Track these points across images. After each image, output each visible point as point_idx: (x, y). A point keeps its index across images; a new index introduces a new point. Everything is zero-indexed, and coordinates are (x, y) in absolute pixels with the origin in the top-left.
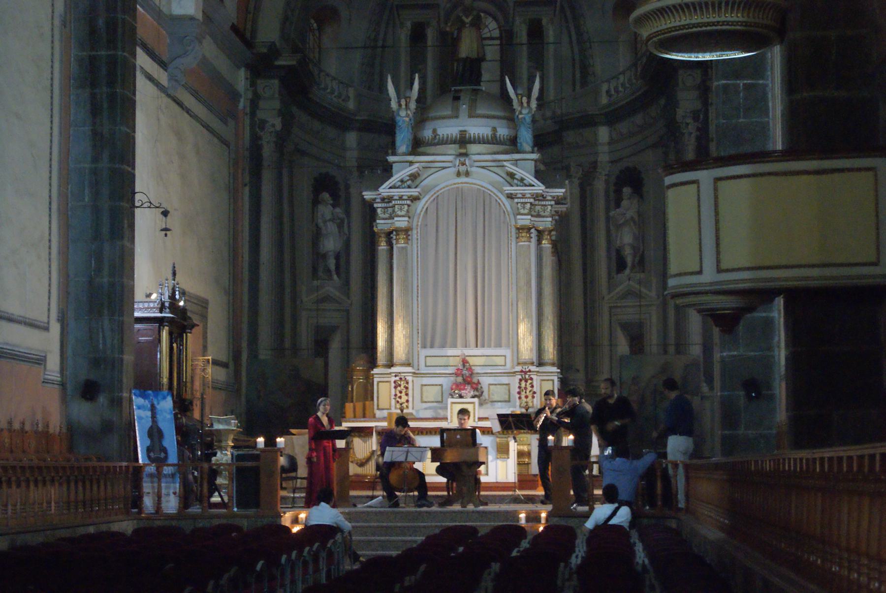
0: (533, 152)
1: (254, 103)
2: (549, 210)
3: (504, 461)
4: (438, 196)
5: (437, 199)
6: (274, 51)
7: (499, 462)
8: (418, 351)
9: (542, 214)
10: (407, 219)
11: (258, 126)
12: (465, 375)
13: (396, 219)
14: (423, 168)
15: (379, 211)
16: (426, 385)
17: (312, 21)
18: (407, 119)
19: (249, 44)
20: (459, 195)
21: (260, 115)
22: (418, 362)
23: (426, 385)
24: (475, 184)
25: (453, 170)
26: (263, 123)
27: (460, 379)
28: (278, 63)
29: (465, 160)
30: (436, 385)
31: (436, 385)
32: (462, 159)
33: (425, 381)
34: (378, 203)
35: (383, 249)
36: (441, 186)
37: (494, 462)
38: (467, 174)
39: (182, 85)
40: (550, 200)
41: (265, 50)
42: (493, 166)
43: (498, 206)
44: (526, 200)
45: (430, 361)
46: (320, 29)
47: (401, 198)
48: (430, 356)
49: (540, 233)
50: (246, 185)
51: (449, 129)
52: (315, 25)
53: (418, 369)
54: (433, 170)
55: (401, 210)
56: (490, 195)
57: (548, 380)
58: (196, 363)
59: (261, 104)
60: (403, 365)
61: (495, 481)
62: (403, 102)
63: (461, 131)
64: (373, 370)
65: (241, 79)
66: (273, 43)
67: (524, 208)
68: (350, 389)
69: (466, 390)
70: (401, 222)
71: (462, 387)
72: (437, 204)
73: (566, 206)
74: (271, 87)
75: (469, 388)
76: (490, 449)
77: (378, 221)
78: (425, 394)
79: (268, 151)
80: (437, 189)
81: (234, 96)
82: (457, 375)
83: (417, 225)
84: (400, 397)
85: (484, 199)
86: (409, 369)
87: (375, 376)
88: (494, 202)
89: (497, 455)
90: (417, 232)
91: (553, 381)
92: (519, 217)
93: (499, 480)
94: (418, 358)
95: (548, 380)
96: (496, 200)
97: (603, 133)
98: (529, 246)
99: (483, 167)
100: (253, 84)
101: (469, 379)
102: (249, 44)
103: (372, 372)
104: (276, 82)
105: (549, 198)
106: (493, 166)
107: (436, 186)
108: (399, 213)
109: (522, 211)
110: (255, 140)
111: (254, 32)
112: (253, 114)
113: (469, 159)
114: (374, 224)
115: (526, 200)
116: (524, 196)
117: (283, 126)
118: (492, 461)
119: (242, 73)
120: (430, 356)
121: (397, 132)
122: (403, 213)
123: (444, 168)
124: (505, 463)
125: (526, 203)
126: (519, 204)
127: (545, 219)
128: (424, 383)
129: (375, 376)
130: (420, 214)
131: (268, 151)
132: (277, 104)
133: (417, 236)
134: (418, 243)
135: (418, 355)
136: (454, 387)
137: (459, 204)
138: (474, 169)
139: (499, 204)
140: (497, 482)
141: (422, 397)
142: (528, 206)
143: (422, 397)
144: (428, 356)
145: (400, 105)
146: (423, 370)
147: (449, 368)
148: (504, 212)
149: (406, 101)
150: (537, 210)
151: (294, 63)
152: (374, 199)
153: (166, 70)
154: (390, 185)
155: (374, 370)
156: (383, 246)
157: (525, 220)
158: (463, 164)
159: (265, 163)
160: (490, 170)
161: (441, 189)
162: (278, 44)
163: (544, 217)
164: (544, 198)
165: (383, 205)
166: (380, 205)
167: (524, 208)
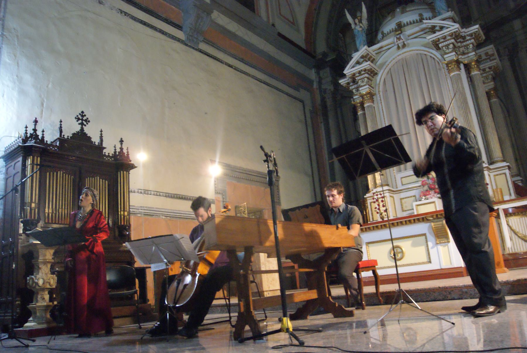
0: (448, 11)
1: (320, 83)
2: (471, 47)
3: (444, 246)
4: (390, 69)
5: (390, 72)
6: (325, 55)
7: (440, 248)
8: (395, 176)
9: (466, 51)
10: (367, 86)
11: (323, 92)
12: (430, 184)
13: (360, 89)
14: (376, 54)
15: (354, 91)
16: (403, 198)
17: (340, 34)
18: (361, 29)
19: (314, 57)
20: (405, 64)
21: (323, 87)
22: (396, 183)
23: (403, 198)
24: (412, 50)
25: (396, 47)
26: (325, 91)
27: (426, 188)
28: (327, 60)
29: (400, 37)
30: (411, 197)
31: (411, 197)
32: (398, 36)
33: (403, 195)
34: (352, 85)
35: (361, 114)
36: (389, 61)
37: (436, 248)
38: (404, 46)
39: (203, 41)
40: (470, 39)
41: (321, 56)
42: (423, 34)
43: (433, 61)
44: (448, 42)
45: (405, 181)
46: (344, 36)
47: (360, 72)
48: (404, 177)
49: (468, 67)
50: (321, 123)
51: (389, 26)
52: (341, 35)
53: (397, 188)
54: (383, 53)
55: (363, 82)
56: (425, 55)
57: (501, 174)
58: (241, 208)
59: (323, 81)
60: (382, 186)
61: (439, 268)
62: (357, 21)
63: (397, 23)
64: (365, 195)
65: (312, 74)
66: (324, 52)
67: (448, 48)
68: (365, 213)
69: (430, 194)
70: (364, 90)
71: (428, 193)
72: (391, 75)
73: (495, 61)
74: (326, 73)
75: (433, 192)
76: (428, 235)
77: (354, 97)
78: (404, 205)
79: (329, 102)
80: (387, 64)
81: (311, 82)
82: (423, 185)
83: (379, 91)
84: (379, 209)
85: (422, 58)
86: (386, 188)
87: (368, 199)
88: (429, 58)
89: (436, 240)
90: (380, 96)
91: (505, 174)
92: (445, 56)
93: (443, 267)
94: (396, 181)
95: (501, 174)
96: (431, 57)
97: (517, 24)
98: (459, 75)
99: (415, 38)
100: (318, 73)
101: (433, 186)
102: (314, 57)
103: (365, 197)
104: (328, 70)
105: (468, 38)
106: (423, 34)
107: (386, 62)
108: (362, 84)
109: (447, 51)
110: (323, 100)
111: (315, 52)
112: (320, 87)
113: (403, 35)
114: (352, 99)
115: (448, 42)
116: (444, 38)
117: (334, 88)
118: (432, 248)
119: (313, 71)
120: (404, 177)
121: (356, 39)
122: (365, 83)
123: (389, 49)
124: (447, 247)
125: (449, 45)
126: (444, 48)
127: (470, 55)
128: (402, 197)
129: (368, 199)
130: (379, 84)
131: (329, 102)
132: (330, 79)
133: (380, 98)
134: (381, 103)
135: (395, 178)
136: (422, 194)
137: (406, 69)
138: (409, 41)
139: (434, 58)
140: (442, 269)
141: (402, 208)
142: (451, 46)
143: (402, 208)
144: (402, 178)
145: (356, 24)
146: (400, 187)
147: (419, 182)
148: (438, 62)
149: (358, 19)
150: (461, 51)
151: (334, 57)
152: (348, 84)
153: (182, 30)
154: (351, 67)
155: (367, 195)
156: (360, 113)
157: (451, 56)
158: (399, 39)
159: (329, 109)
160: (420, 38)
161: (390, 63)
162: (326, 51)
163: (468, 53)
164: (463, 39)
165: (355, 86)
166: (353, 87)
167: (448, 48)
